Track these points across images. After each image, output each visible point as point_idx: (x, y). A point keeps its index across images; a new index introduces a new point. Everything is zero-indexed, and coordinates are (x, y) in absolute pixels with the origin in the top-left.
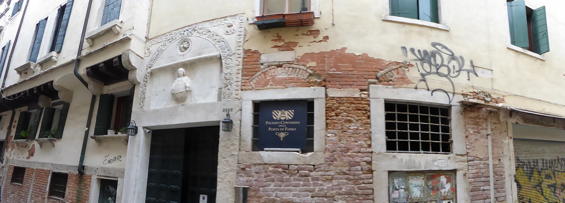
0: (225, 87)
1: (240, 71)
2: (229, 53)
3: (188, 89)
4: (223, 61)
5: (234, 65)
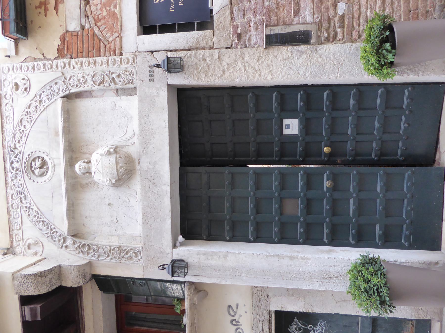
0: (115, 83)
1: (91, 59)
2: (60, 82)
3: (112, 150)
4: (73, 90)
5: (80, 72)
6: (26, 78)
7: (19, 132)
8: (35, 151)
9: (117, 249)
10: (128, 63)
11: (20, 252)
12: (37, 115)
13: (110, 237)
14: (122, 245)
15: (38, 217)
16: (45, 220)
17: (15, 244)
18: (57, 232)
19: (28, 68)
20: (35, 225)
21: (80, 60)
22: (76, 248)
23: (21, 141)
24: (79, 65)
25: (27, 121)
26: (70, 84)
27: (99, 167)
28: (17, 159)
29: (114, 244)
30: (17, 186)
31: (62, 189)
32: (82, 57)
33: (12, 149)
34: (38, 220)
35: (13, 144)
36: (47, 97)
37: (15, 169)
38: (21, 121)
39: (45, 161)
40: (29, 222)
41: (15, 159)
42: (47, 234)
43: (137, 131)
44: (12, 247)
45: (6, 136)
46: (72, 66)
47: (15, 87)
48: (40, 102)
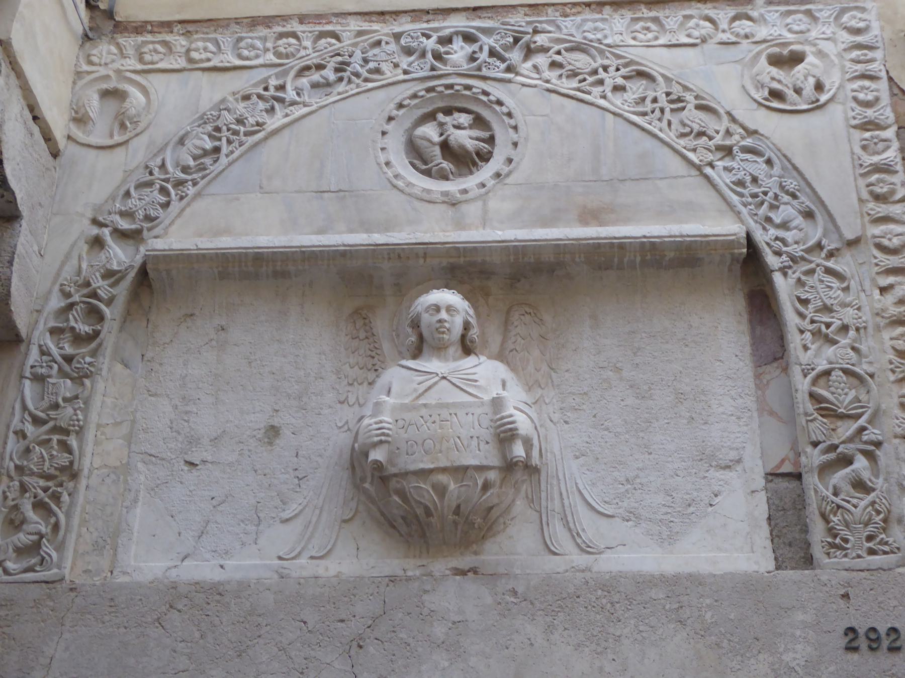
0: (825, 469)
2: (815, 234)
3: (519, 450)
4: (783, 285)
5: (866, 316)
6: (823, 98)
8: (515, 128)
9: (63, 459)
11: (95, 59)
12: (669, 136)
13: (125, 429)
14: (83, 482)
15: (236, 133)
16: (224, 161)
17: (129, 42)
18: (166, 205)
19: (867, 104)
20: (203, 120)
22: (88, 284)
23: (559, 72)
25: (643, 99)
26: (811, 272)
27: (446, 394)
28: (484, 56)
29: (89, 448)
30: (370, 54)
31: (351, 231)
33: (527, 38)
34: (225, 133)
35: (547, 44)
36: (748, 179)
37: (442, 50)
38: (641, 74)
39: (475, 164)
40: (217, 97)
41: (486, 49)
42: (163, 166)
43: (611, 563)
44: (120, 28)
45: (579, 19)
46: (891, 280)
47: (785, 52)
48: (728, 151)
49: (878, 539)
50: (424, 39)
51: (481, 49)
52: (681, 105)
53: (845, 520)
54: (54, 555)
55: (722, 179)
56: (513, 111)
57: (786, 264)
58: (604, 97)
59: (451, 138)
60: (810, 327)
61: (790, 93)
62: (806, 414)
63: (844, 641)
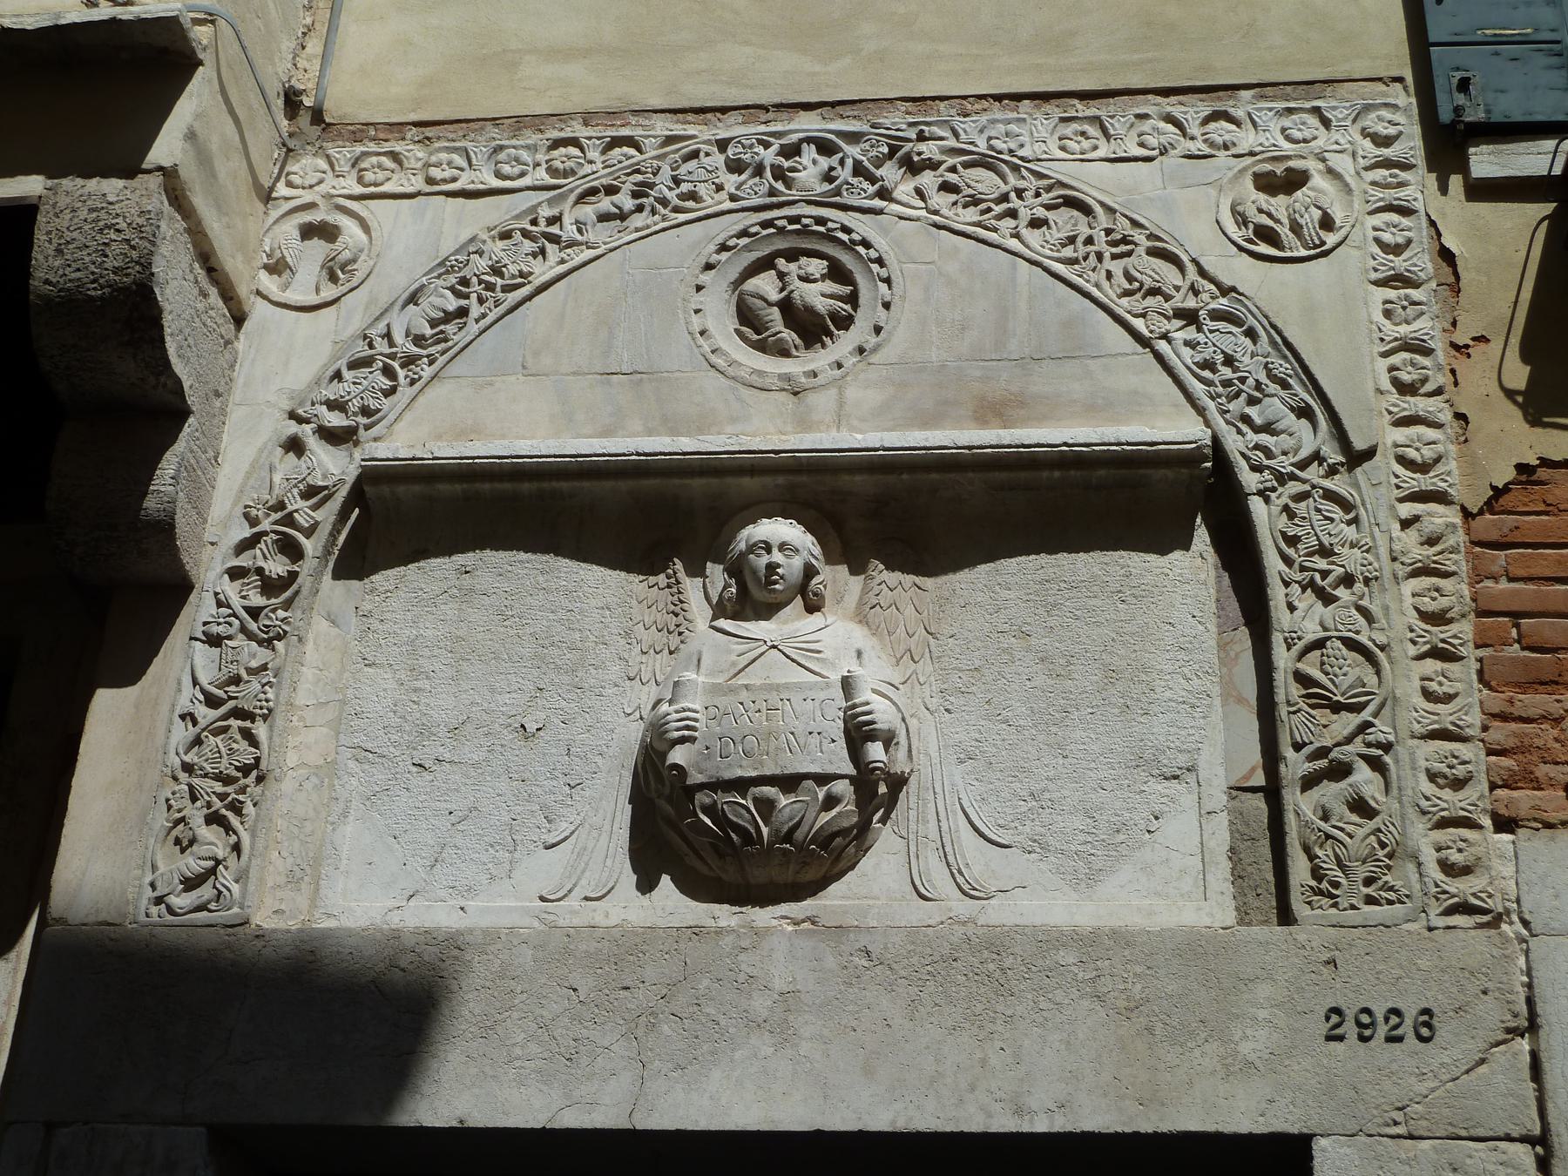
0: (1309, 783)
1: (1463, 630)
7: (1004, 188)
8: (888, 281)
9: (246, 754)
10: (1448, 868)
11: (295, 179)
12: (1108, 294)
13: (330, 713)
15: (490, 287)
16: (473, 328)
17: (343, 153)
18: (391, 391)
19: (1397, 250)
20: (445, 267)
21: (1459, 562)
22: (280, 506)
23: (954, 197)
24: (1419, 553)
25: (1072, 240)
26: (1301, 497)
28: (845, 174)
30: (683, 170)
31: (650, 432)
32: (1478, 576)
33: (908, 147)
34: (476, 287)
35: (938, 157)
36: (1220, 358)
37: (786, 164)
39: (830, 334)
40: (465, 236)
41: (849, 162)
42: (388, 335)
43: (998, 913)
45: (984, 118)
46: (1418, 508)
48: (1189, 317)
49: (1380, 883)
50: (760, 149)
51: (842, 162)
52: (1123, 248)
53: (1337, 856)
54: (235, 888)
55: (1183, 358)
56: (884, 256)
57: (1268, 484)
58: (1017, 236)
59: (796, 295)
60: (1298, 576)
61: (1284, 231)
62: (1289, 703)
63: (1324, 1028)
